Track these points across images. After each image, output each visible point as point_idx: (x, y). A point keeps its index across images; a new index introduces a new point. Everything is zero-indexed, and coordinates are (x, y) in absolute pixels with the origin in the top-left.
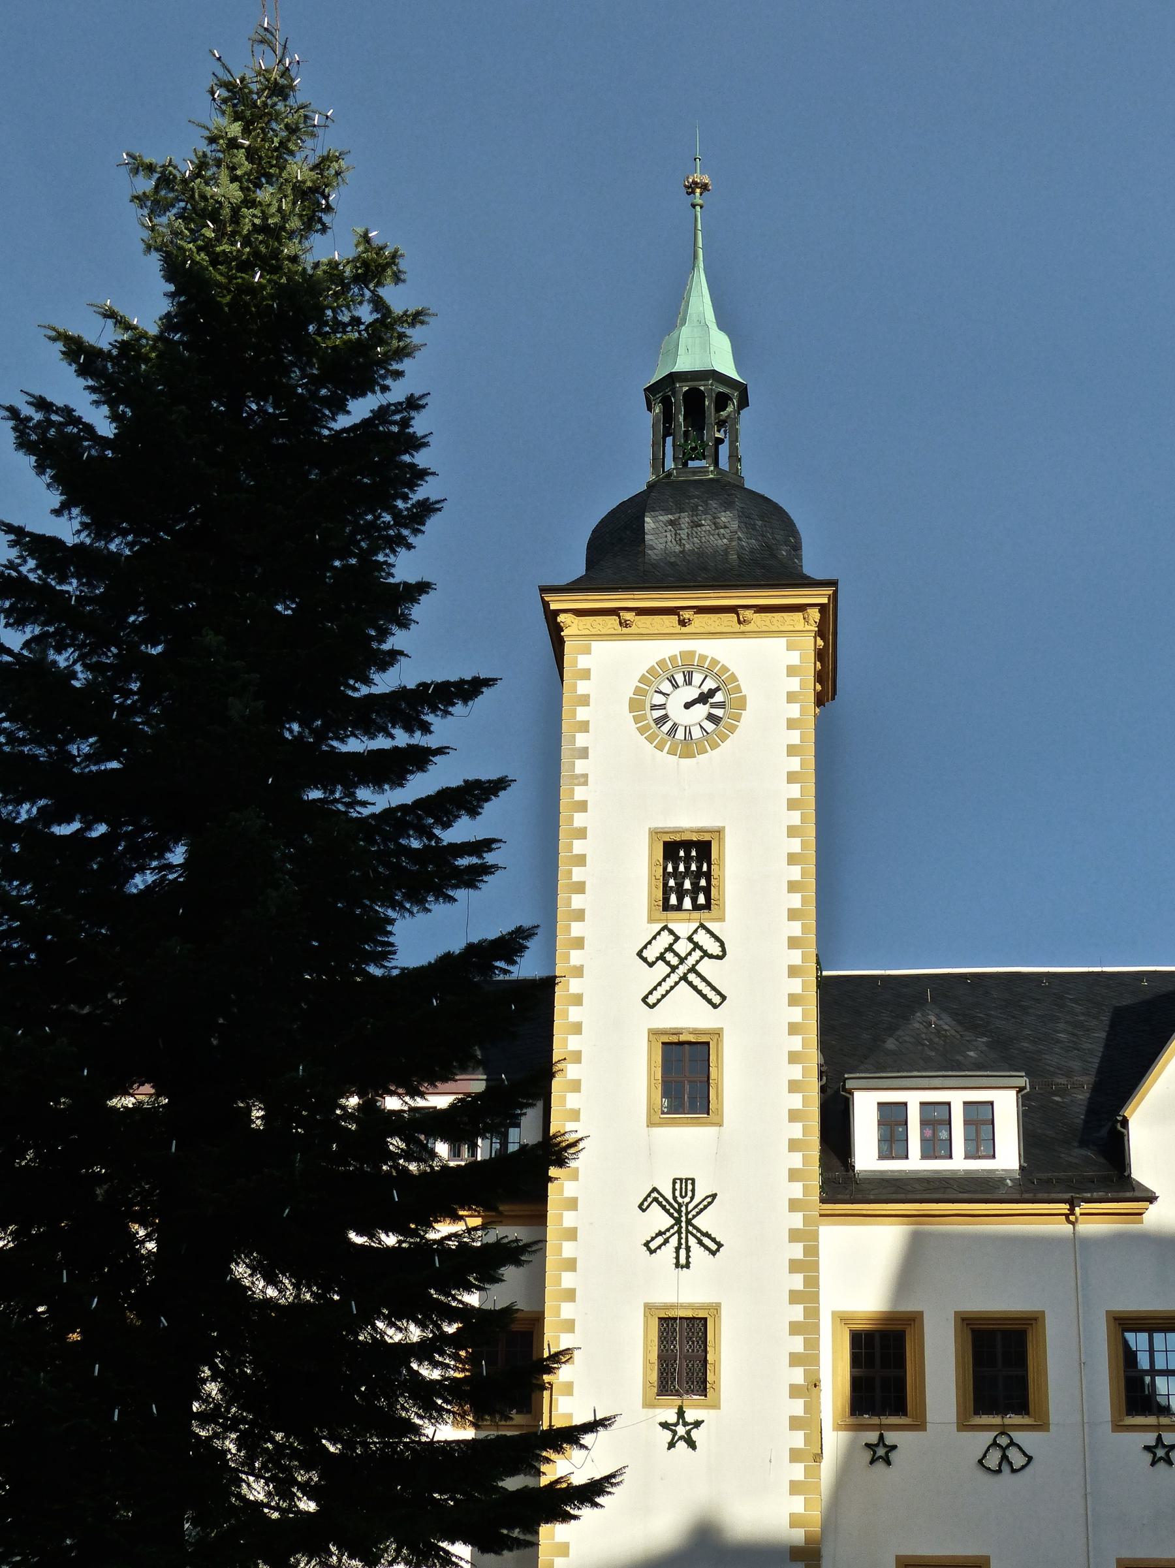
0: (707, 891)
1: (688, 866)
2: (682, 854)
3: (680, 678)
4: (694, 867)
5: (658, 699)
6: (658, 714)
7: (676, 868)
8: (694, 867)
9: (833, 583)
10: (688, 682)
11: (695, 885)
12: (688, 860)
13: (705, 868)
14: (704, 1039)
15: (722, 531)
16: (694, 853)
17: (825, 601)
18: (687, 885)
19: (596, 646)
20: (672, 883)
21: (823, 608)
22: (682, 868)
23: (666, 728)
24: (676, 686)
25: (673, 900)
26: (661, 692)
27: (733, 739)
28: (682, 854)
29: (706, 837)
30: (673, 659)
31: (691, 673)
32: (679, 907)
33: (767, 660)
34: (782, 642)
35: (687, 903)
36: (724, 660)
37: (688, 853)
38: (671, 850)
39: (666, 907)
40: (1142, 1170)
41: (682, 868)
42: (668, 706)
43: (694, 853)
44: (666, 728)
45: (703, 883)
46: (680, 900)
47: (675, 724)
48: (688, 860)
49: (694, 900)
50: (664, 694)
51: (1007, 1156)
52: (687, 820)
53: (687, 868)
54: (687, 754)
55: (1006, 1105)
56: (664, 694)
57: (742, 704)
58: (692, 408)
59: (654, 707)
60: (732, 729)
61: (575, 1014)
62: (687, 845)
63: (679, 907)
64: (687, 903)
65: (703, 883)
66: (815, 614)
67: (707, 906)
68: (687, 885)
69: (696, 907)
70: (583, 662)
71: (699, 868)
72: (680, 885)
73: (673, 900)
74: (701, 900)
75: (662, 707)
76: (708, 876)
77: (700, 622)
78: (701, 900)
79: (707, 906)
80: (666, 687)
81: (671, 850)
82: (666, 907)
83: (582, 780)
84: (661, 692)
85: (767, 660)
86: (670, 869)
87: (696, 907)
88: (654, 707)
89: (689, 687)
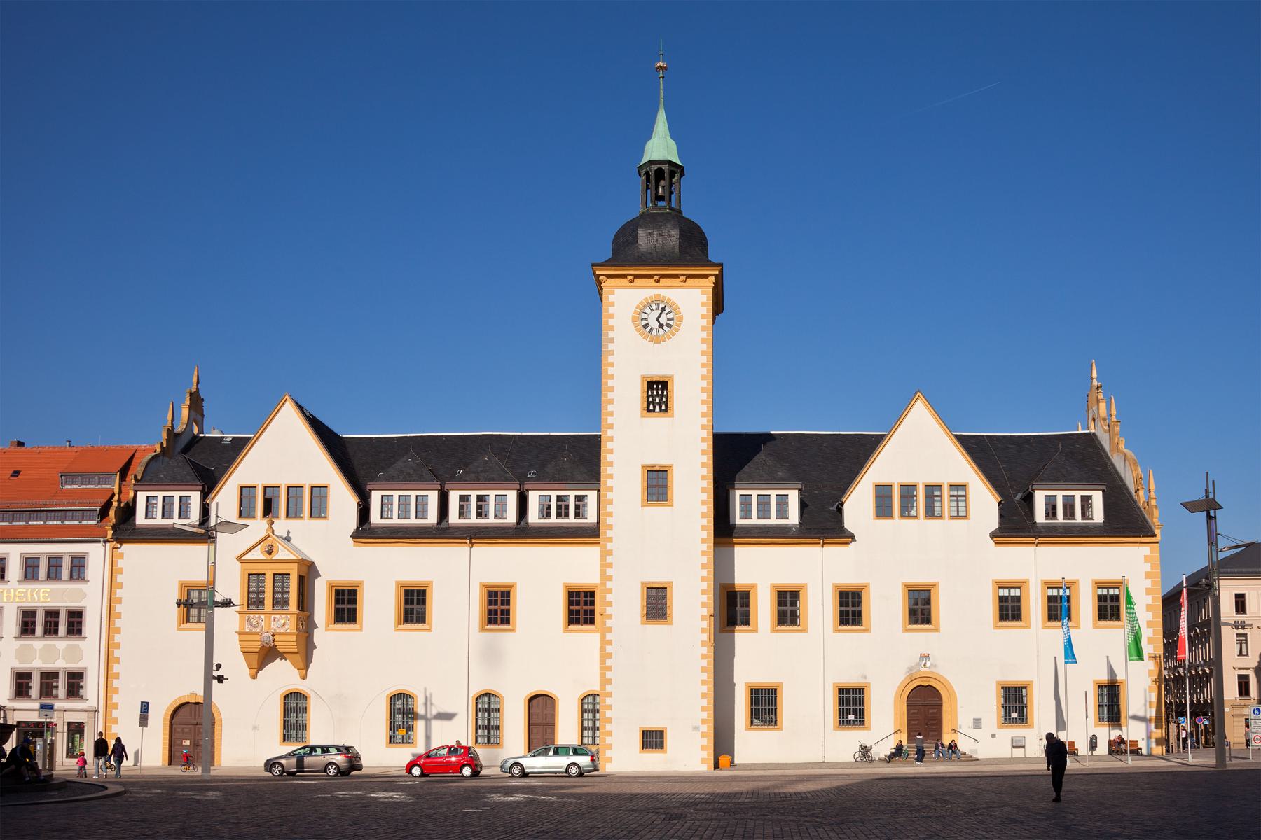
1: (657, 393)
5: (644, 316)
9: (721, 265)
12: (657, 389)
19: (617, 291)
21: (715, 276)
27: (678, 335)
33: (691, 299)
34: (699, 291)
35: (657, 409)
36: (673, 299)
38: (650, 385)
39: (648, 411)
40: (849, 524)
51: (793, 518)
52: (657, 372)
54: (658, 342)
55: (793, 497)
57: (681, 319)
60: (677, 331)
61: (610, 458)
62: (657, 383)
64: (657, 409)
66: (712, 279)
67: (666, 411)
69: (661, 411)
72: (653, 402)
77: (664, 281)
79: (666, 411)
80: (648, 310)
81: (650, 385)
82: (648, 411)
85: (691, 299)
87: (661, 411)
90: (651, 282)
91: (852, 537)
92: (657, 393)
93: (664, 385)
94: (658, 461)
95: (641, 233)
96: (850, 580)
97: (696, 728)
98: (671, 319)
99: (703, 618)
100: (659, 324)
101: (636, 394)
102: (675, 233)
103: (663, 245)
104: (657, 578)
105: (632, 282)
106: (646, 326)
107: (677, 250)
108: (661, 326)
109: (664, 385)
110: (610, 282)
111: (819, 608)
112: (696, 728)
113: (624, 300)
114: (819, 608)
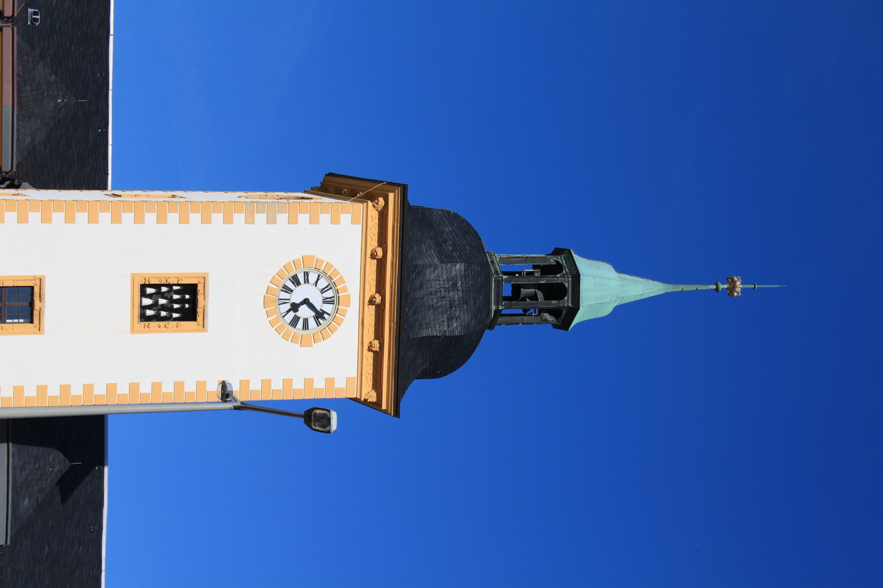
0: (157, 318)
1: (175, 303)
2: (187, 297)
3: (329, 294)
4: (176, 306)
5: (313, 277)
6: (301, 278)
7: (177, 292)
8: (176, 306)
9: (397, 414)
10: (326, 301)
12: (181, 301)
13: (175, 315)
14: (36, 319)
15: (446, 324)
17: (384, 407)
18: (162, 301)
19: (358, 228)
20: (164, 289)
22: (176, 297)
23: (290, 285)
25: (150, 291)
26: (318, 279)
28: (187, 297)
29: (200, 318)
30: (345, 289)
31: (332, 302)
34: (353, 373)
35: (147, 302)
37: (187, 301)
38: (191, 290)
41: (176, 297)
42: (307, 285)
43: (187, 306)
44: (290, 285)
45: (163, 314)
46: (150, 296)
47: (292, 291)
48: (181, 301)
49: (149, 307)
50: (317, 282)
52: (212, 302)
53: (177, 301)
56: (317, 282)
58: (556, 291)
59: (306, 274)
60: (285, 337)
62: (194, 302)
63: (143, 294)
64: (147, 302)
65: (163, 314)
66: (373, 398)
67: (144, 318)
68: (162, 301)
69: (143, 308)
70: (346, 218)
71: (176, 311)
73: (150, 291)
74: (149, 313)
75: (307, 281)
77: (371, 311)
78: (149, 313)
79: (144, 318)
80: (323, 283)
81: (191, 290)
82: (143, 287)
84: (318, 279)
86: (175, 288)
87: (143, 308)
88: (306, 274)
89: (321, 301)
90: (371, 290)
92: (175, 303)
93: (190, 313)
94: (50, 306)
95: (459, 267)
98: (306, 326)
100: (301, 309)
101: (174, 267)
102: (456, 328)
103: (430, 307)
105: (373, 256)
106: (295, 280)
107: (425, 333)
108: (295, 307)
109: (190, 313)
110: (374, 215)
113: (341, 239)
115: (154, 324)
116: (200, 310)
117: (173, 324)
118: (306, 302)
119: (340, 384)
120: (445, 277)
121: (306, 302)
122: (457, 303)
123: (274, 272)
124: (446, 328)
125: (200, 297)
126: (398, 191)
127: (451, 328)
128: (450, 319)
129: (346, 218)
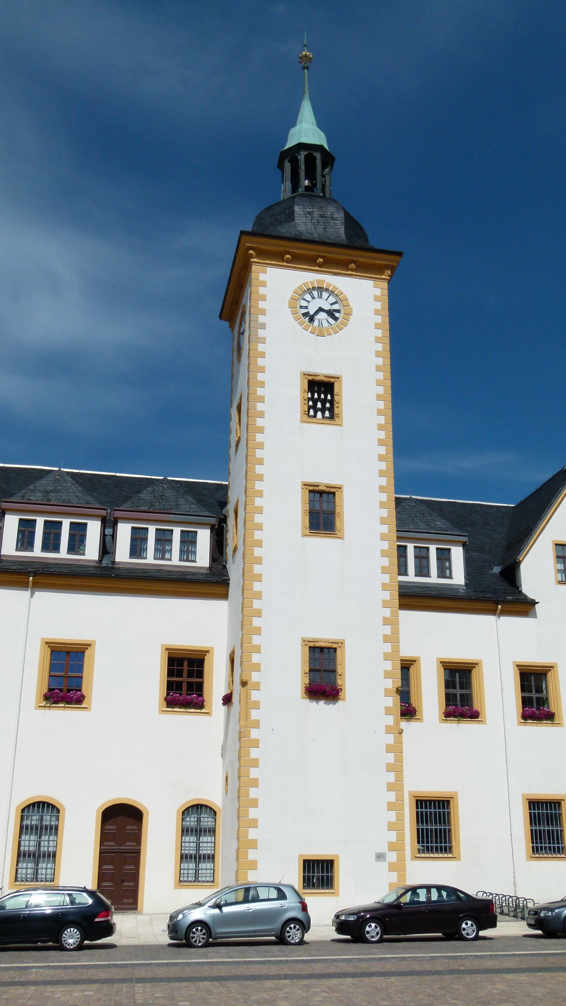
0: (331, 410)
1: (321, 394)
2: (316, 388)
5: (304, 303)
8: (322, 396)
9: (400, 254)
11: (323, 404)
13: (329, 397)
14: (333, 490)
16: (323, 389)
18: (319, 405)
19: (269, 270)
22: (316, 396)
24: (313, 298)
26: (305, 300)
28: (316, 388)
30: (312, 283)
32: (315, 416)
34: (370, 283)
35: (319, 414)
41: (316, 396)
42: (309, 308)
43: (323, 389)
45: (328, 405)
49: (323, 414)
50: (307, 301)
51: (458, 576)
52: (322, 370)
53: (319, 396)
54: (321, 335)
56: (307, 301)
59: (301, 307)
65: (328, 405)
67: (332, 417)
68: (319, 405)
70: (262, 277)
71: (326, 397)
75: (306, 308)
76: (332, 402)
78: (327, 414)
79: (332, 417)
83: (263, 340)
84: (305, 300)
88: (301, 307)
89: (320, 299)
91: (533, 603)
94: (324, 478)
95: (297, 208)
96: (534, 658)
97: (380, 857)
99: (387, 693)
104: (324, 634)
107: (343, 236)
111: (498, 693)
112: (380, 857)
113: (276, 286)
114: (498, 693)
115: (336, 411)
116: (326, 379)
117: (336, 398)
118: (321, 310)
119: (378, 292)
120: (304, 219)
121: (321, 310)
122: (322, 213)
123: (300, 328)
124: (339, 222)
125: (317, 378)
126: (244, 238)
127: (339, 219)
128: (333, 219)
129: (262, 277)
